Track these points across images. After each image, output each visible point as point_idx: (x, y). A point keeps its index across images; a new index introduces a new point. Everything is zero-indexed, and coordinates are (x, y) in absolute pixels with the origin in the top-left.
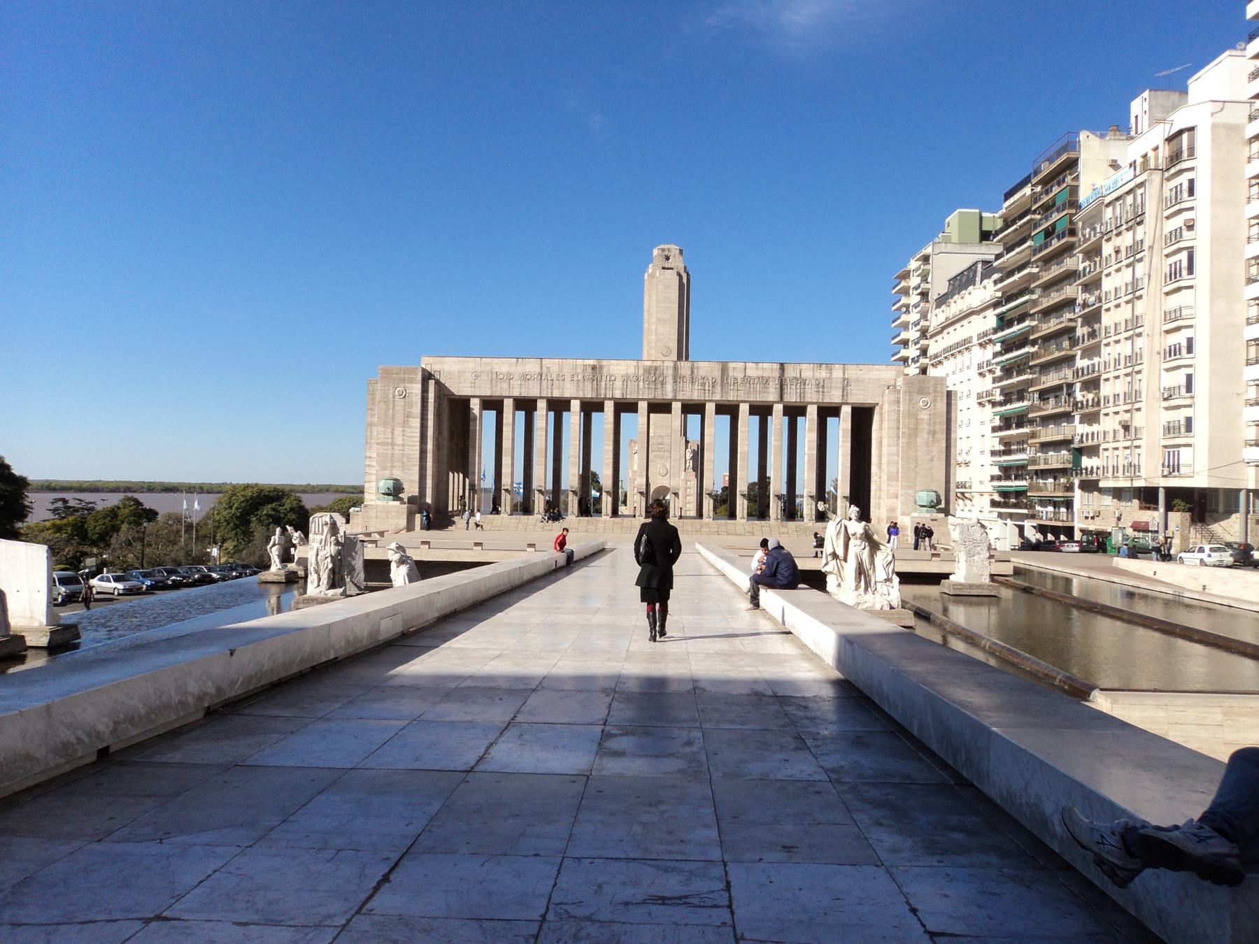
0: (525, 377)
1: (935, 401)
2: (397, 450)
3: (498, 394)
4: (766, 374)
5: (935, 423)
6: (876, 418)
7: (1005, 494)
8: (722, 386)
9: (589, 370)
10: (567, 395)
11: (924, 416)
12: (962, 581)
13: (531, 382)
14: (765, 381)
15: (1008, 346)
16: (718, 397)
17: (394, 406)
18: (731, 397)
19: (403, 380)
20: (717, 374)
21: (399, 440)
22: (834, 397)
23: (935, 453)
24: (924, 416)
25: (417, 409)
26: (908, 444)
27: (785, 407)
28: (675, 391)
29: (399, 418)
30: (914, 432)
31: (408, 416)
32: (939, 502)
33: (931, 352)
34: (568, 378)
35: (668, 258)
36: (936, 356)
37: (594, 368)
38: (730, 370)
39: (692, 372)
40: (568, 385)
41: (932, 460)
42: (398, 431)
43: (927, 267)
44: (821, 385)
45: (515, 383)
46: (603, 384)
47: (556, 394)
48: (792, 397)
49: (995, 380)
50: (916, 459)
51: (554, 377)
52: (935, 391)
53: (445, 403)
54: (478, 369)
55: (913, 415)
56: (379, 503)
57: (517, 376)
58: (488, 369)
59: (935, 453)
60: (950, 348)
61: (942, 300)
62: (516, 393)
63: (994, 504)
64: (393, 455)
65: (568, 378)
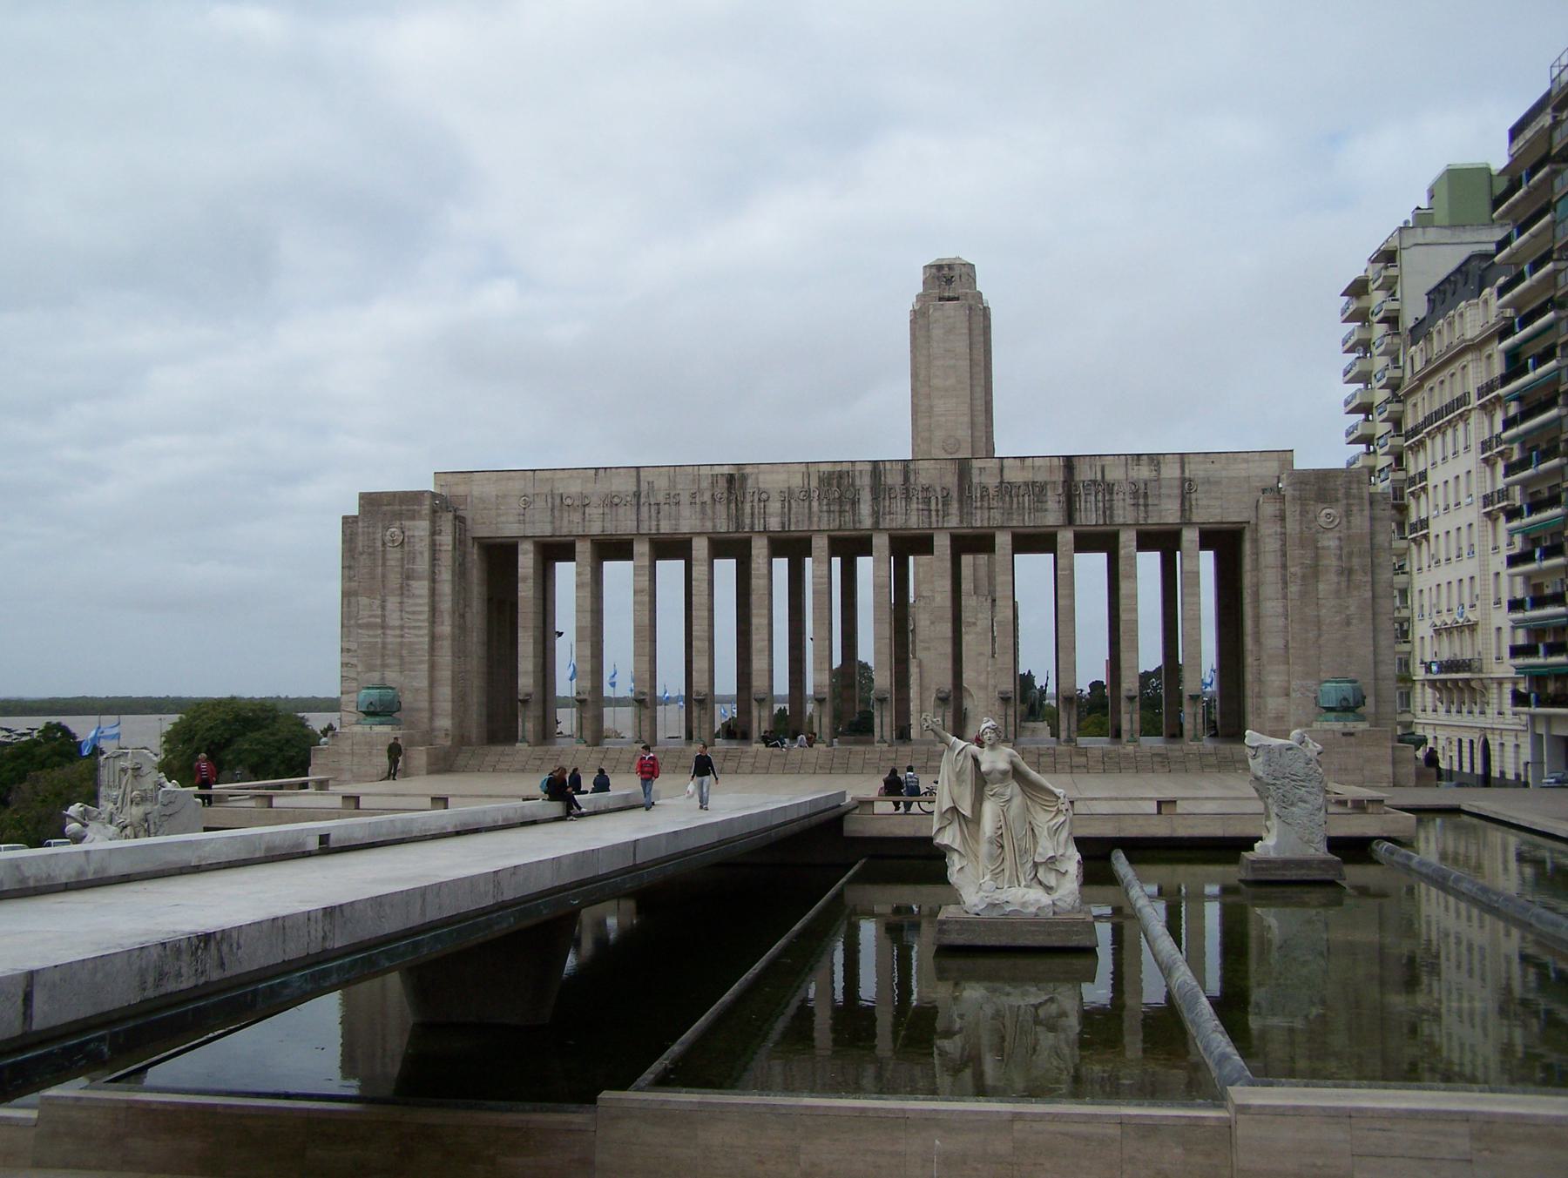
0: (611, 502)
1: (1348, 513)
2: (392, 638)
3: (565, 531)
4: (1041, 477)
5: (1350, 554)
6: (1247, 547)
7: (1538, 678)
8: (960, 501)
9: (723, 483)
10: (685, 529)
11: (1330, 542)
12: (1273, 855)
13: (621, 510)
14: (1038, 490)
15: (1531, 404)
16: (953, 521)
17: (384, 559)
18: (979, 521)
19: (399, 516)
20: (951, 480)
21: (394, 619)
22: (1167, 513)
23: (1353, 609)
24: (1330, 542)
25: (423, 565)
26: (1303, 595)
27: (1077, 535)
28: (876, 514)
29: (394, 580)
30: (1314, 572)
31: (408, 576)
32: (1361, 701)
33: (1409, 424)
34: (685, 498)
35: (949, 281)
36: (1415, 431)
37: (730, 479)
38: (975, 472)
39: (906, 479)
40: (686, 511)
41: (1348, 624)
42: (392, 602)
43: (1392, 272)
44: (1141, 494)
45: (594, 512)
46: (748, 509)
47: (666, 527)
48: (1089, 517)
49: (1510, 469)
50: (1318, 623)
51: (661, 498)
52: (1348, 495)
53: (474, 554)
54: (530, 491)
55: (1309, 542)
56: (358, 728)
57: (595, 500)
58: (547, 489)
59: (1353, 609)
60: (1438, 415)
61: (1420, 331)
62: (595, 529)
63: (1519, 699)
64: (384, 647)
65: (685, 498)
